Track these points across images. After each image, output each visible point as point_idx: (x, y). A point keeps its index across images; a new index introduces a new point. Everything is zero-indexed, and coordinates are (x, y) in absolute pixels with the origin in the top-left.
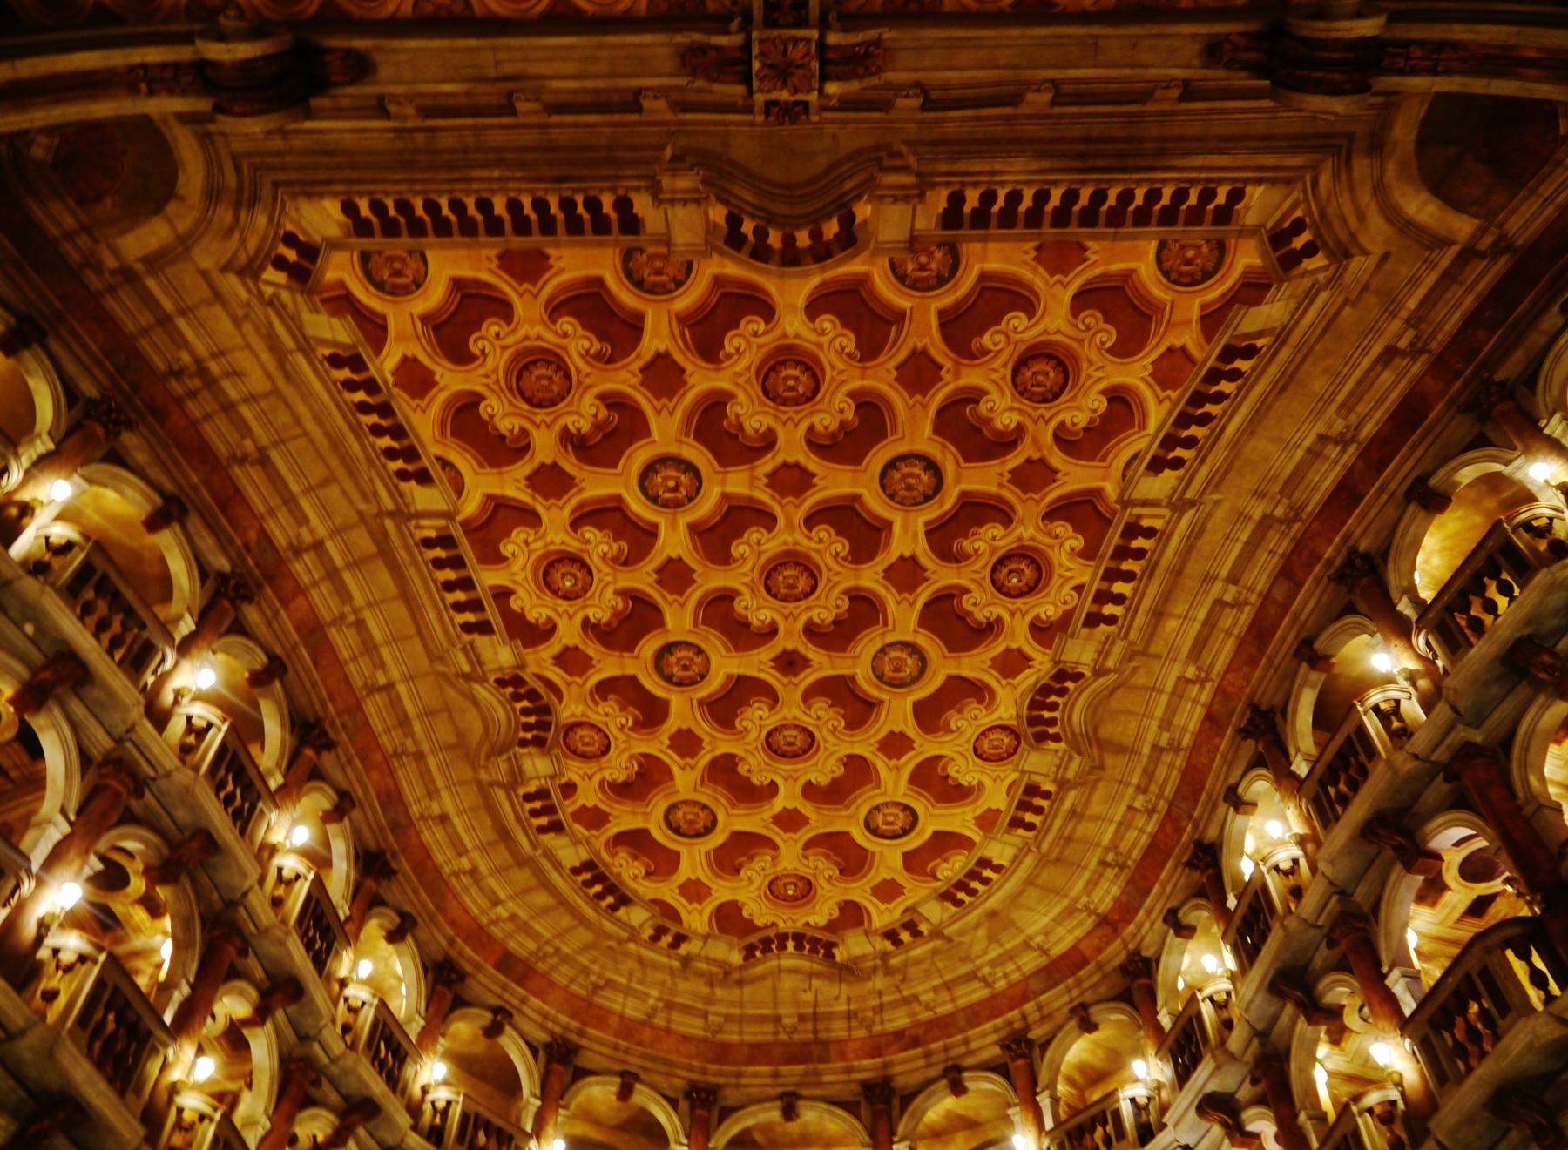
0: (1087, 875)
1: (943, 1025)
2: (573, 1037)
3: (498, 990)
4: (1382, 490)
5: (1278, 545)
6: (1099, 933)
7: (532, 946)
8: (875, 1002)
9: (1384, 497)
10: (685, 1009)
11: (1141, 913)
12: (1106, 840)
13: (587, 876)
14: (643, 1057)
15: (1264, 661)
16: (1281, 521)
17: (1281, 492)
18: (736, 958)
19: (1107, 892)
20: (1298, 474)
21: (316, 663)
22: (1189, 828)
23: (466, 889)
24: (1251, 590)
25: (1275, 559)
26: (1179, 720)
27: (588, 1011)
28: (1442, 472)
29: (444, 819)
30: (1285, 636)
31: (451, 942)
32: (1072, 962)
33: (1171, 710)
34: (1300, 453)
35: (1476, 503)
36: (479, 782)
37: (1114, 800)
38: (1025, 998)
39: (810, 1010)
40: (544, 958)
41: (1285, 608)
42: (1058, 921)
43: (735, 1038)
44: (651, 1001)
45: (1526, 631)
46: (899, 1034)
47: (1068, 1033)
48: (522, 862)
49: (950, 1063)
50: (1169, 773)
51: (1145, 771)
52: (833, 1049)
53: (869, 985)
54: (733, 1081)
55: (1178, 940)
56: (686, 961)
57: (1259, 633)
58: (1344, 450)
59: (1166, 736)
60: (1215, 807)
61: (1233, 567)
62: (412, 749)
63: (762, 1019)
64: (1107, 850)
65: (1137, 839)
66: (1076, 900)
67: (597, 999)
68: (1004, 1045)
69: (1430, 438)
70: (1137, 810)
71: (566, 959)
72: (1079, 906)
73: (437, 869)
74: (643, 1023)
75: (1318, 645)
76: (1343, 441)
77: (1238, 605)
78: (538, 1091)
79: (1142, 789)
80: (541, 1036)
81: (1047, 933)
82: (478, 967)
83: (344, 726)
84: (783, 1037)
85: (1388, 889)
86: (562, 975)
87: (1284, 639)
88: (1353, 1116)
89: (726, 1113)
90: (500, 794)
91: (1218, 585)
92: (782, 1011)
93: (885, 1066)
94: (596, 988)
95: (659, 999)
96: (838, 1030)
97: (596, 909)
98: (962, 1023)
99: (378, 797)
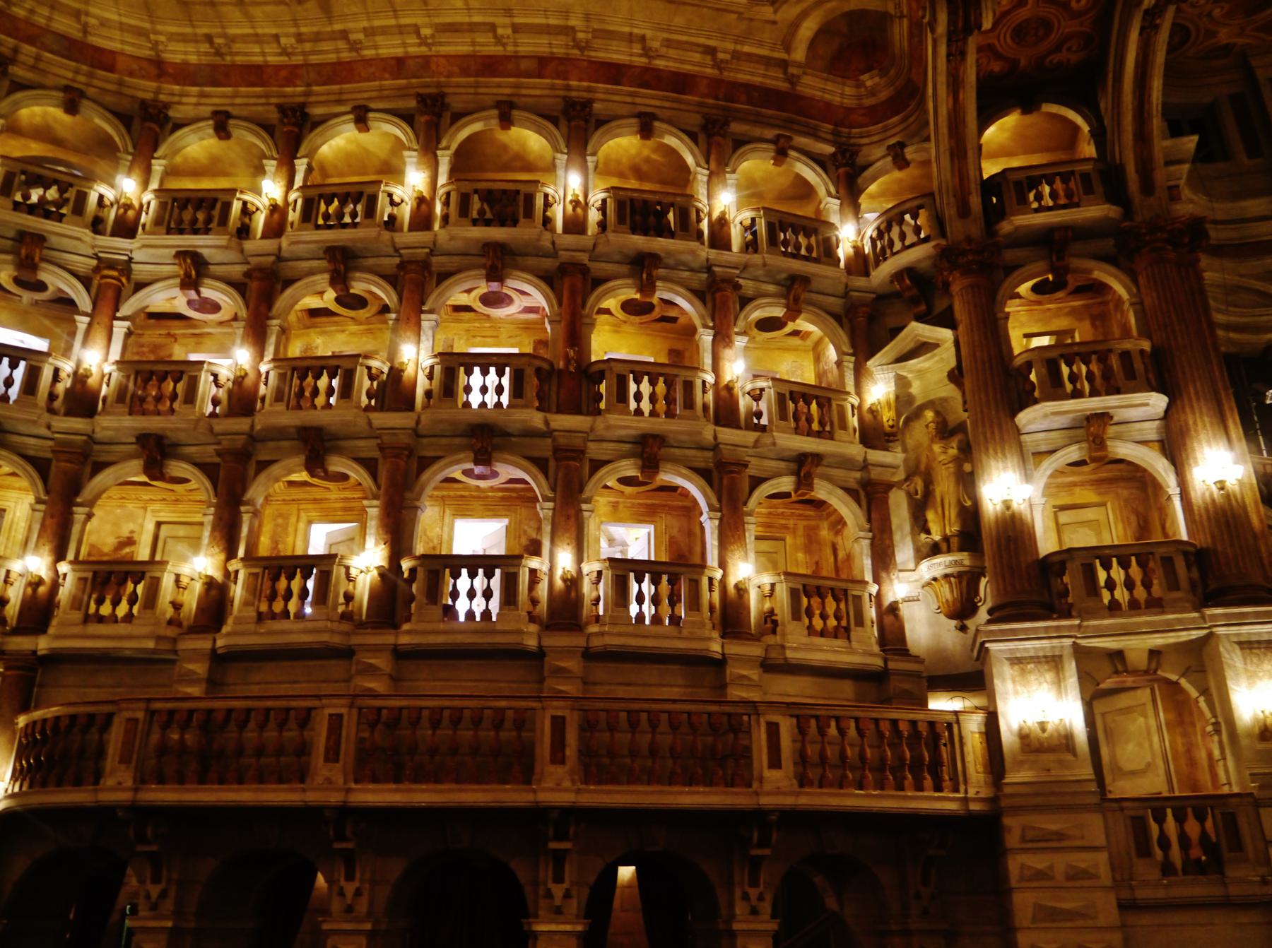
0: (188, 30)
4: (631, 94)
5: (558, 46)
6: (145, 65)
9: (629, 99)
11: (195, 89)
12: (232, 31)
15: (472, 79)
16: (574, 39)
17: (595, 30)
19: (186, 53)
20: (610, 35)
22: (299, 89)
24: (516, 44)
25: (547, 50)
26: (380, 40)
28: (665, 126)
30: (502, 86)
32: (103, 60)
33: (384, 31)
34: (627, 29)
35: (655, 151)
37: (275, 22)
38: (31, 40)
41: (518, 75)
42: (122, 27)
45: (662, 255)
47: (51, 97)
50: (329, 53)
51: (318, 33)
55: (211, 131)
57: (490, 66)
58: (641, 56)
59: (361, 36)
60: (339, 102)
61: (526, 25)
64: (225, 36)
65: (253, 54)
66: (157, 33)
69: (675, 105)
70: (279, 42)
72: (152, 37)
75: (515, 113)
76: (646, 52)
77: (499, 40)
79: (300, 38)
81: (104, 23)
85: (463, 275)
87: (499, 86)
88: (357, 363)
91: (507, 20)
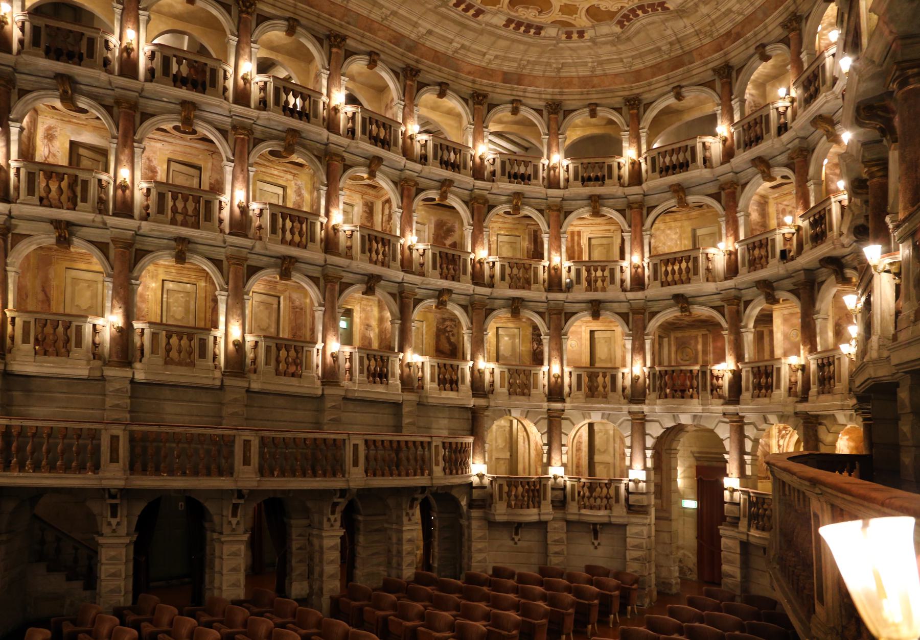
1: (749, 21)
2: (558, 97)
3: (509, 92)
7: (515, 65)
8: (709, 21)
10: (609, 61)
13: (513, 26)
14: (597, 92)
18: (617, 29)
21: (311, 6)
23: (466, 55)
27: (559, 82)
29: (430, 32)
31: (474, 82)
36: (430, 10)
39: (674, 38)
40: (524, 67)
43: (641, 66)
44: (590, 64)
46: (728, 34)
48: (481, 32)
49: (758, 44)
52: (694, 53)
53: (699, 14)
54: (647, 88)
56: (593, 40)
62: (389, 13)
63: (651, 52)
67: (563, 74)
68: (784, 25)
71: (536, 63)
73: (444, 54)
74: (591, 77)
78: (546, 131)
80: (541, 104)
82: (494, 86)
83: (348, 23)
84: (666, 57)
86: (538, 71)
89: (648, 105)
90: (443, 10)
92: (659, 44)
93: (726, 54)
94: (559, 70)
95: (593, 62)
96: (694, 42)
97: (530, 37)
98: (760, 15)
99: (391, 42)
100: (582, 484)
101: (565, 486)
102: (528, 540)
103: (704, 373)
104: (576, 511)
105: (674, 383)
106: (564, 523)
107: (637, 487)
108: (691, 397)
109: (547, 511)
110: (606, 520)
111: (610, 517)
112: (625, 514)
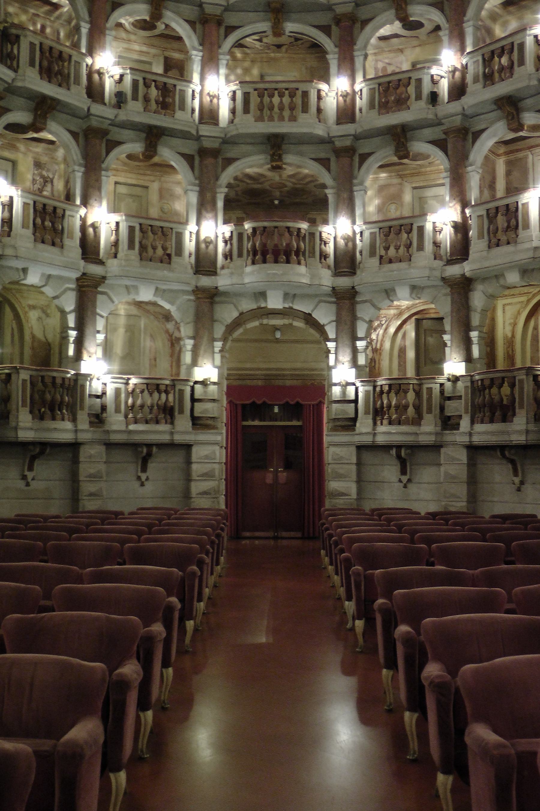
100: (131, 387)
101: (104, 393)
102: (48, 476)
103: (312, 235)
104: (123, 428)
105: (271, 250)
106: (103, 448)
107: (205, 392)
108: (299, 263)
109: (84, 429)
110: (166, 438)
111: (172, 433)
112: (191, 429)
